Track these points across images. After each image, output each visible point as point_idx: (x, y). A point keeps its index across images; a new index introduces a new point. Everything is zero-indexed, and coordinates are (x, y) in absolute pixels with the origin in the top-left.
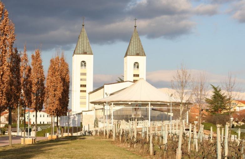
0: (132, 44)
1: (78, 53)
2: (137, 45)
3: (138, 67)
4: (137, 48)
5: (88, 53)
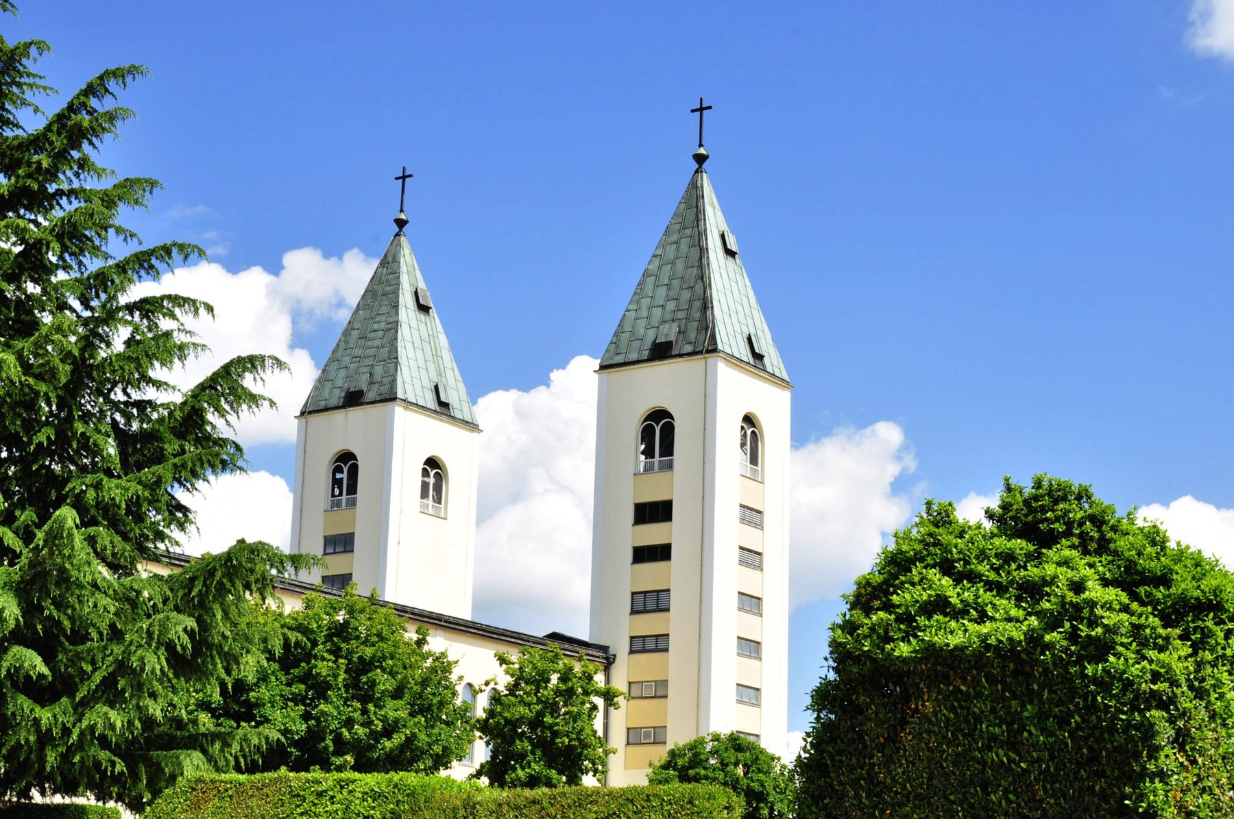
0: (651, 280)
1: (323, 404)
2: (676, 283)
3: (668, 449)
4: (671, 306)
5: (370, 396)
